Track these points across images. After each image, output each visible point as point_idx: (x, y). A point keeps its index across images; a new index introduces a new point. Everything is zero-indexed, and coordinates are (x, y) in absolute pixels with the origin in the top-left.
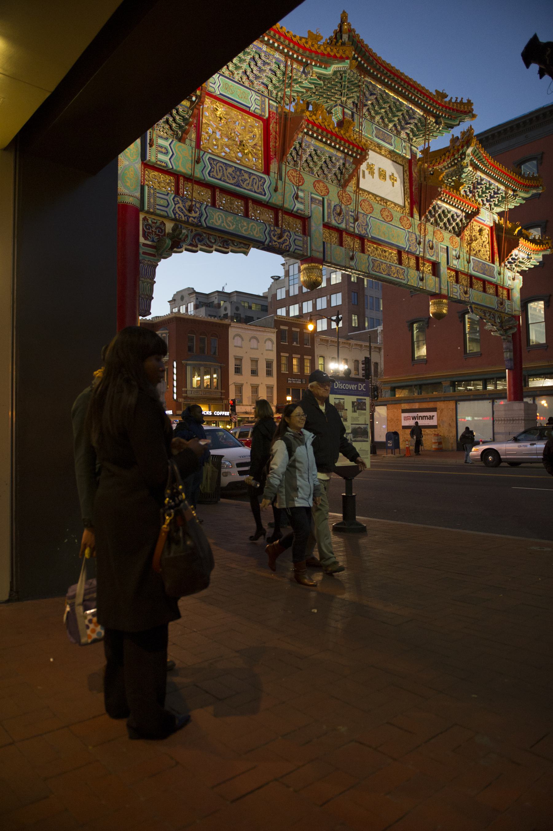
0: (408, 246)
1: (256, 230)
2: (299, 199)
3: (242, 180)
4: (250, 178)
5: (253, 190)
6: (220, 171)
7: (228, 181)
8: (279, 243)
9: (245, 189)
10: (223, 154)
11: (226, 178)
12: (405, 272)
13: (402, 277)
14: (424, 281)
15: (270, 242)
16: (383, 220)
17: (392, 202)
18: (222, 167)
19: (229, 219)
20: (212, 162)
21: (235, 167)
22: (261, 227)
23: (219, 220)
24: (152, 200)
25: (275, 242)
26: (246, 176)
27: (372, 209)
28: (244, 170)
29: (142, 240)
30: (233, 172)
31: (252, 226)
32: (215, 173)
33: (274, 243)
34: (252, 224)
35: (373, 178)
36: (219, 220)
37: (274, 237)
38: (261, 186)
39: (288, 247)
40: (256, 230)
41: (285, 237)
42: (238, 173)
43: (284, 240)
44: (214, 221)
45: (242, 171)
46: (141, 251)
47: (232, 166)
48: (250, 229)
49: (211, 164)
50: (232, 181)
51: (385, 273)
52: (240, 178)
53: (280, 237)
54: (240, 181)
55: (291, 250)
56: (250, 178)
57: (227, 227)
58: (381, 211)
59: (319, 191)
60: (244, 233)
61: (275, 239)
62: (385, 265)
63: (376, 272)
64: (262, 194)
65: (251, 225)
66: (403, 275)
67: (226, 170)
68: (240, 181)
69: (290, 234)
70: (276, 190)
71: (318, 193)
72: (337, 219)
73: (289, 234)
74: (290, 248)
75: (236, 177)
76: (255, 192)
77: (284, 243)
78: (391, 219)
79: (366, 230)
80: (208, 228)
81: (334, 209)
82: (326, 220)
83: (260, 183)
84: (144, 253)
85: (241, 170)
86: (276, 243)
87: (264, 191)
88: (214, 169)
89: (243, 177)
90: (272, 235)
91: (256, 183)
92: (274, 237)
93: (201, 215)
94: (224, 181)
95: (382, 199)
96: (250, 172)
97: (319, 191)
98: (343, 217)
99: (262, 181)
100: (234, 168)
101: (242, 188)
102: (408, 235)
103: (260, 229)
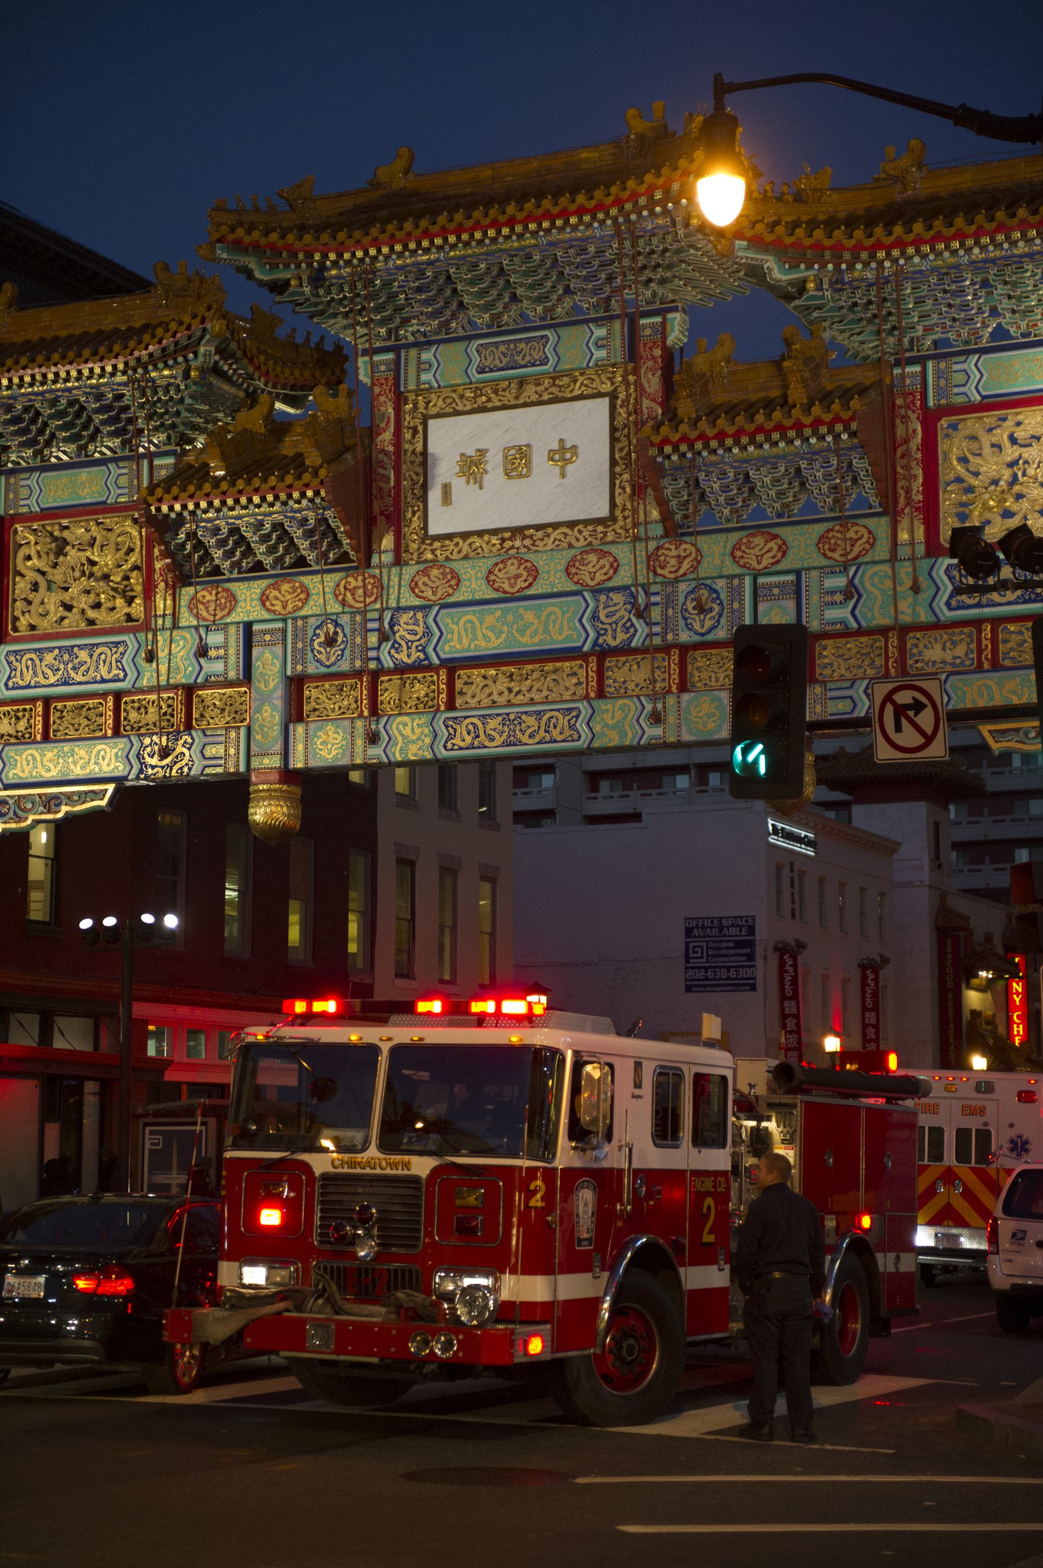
0: (592, 635)
1: (107, 760)
2: (212, 653)
3: (74, 668)
4: (91, 656)
5: (99, 678)
6: (28, 668)
7: (43, 682)
8: (162, 767)
9: (80, 683)
11: (41, 679)
12: (577, 717)
13: (567, 733)
14: (671, 719)
15: (141, 771)
16: (501, 595)
18: (31, 659)
19: (49, 755)
20: (12, 658)
21: (60, 648)
22: (121, 746)
23: (28, 765)
25: (153, 767)
26: (83, 655)
27: (453, 582)
28: (78, 646)
30: (55, 659)
31: (99, 752)
32: (17, 680)
33: (150, 771)
34: (99, 747)
35: (481, 488)
36: (28, 765)
37: (152, 757)
38: (117, 662)
39: (186, 770)
40: (107, 760)
41: (180, 749)
42: (66, 657)
43: (177, 757)
44: (18, 771)
45: (76, 650)
47: (54, 648)
48: (93, 761)
49: (9, 663)
50: (53, 680)
51: (499, 741)
52: (70, 665)
53: (163, 757)
54: (70, 671)
55: (192, 773)
56: (91, 656)
57: (43, 773)
58: (490, 572)
59: (278, 607)
61: (154, 761)
62: (500, 718)
63: (461, 748)
64: (119, 680)
65: (95, 752)
66: (572, 727)
67: (41, 660)
68: (70, 671)
69: (192, 738)
71: (274, 612)
72: (323, 657)
73: (190, 740)
74: (190, 769)
75: (62, 666)
76: (104, 681)
77: (176, 763)
78: (531, 579)
79: (423, 651)
81: (315, 635)
83: (115, 656)
85: (73, 647)
86: (156, 770)
87: (124, 670)
88: (15, 670)
89: (76, 661)
90: (146, 756)
91: (104, 662)
92: (152, 757)
94: (35, 687)
96: (91, 645)
97: (278, 607)
98: (342, 647)
99: (121, 649)
100: (57, 651)
101: (74, 684)
102: (592, 604)
103: (116, 754)
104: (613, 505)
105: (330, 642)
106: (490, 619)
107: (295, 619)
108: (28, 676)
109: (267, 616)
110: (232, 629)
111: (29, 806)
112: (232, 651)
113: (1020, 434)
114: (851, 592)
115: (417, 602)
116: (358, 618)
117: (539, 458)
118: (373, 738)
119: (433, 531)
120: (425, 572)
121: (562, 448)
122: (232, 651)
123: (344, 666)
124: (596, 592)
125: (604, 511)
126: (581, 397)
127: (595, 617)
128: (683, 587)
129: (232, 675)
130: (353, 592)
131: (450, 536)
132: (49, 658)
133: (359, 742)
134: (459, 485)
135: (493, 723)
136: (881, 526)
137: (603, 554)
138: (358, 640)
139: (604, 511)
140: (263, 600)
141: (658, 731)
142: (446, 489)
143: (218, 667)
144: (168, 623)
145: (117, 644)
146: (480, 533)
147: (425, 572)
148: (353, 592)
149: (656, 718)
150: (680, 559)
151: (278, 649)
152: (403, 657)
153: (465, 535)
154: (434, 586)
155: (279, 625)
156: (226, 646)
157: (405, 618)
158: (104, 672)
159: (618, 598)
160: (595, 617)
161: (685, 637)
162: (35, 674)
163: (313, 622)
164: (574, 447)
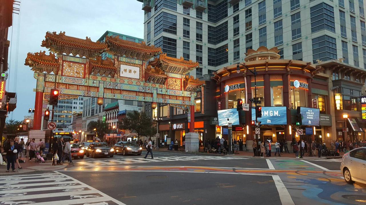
10: (70, 75)
14: (145, 99)
17: (134, 78)
24: (47, 90)
26: (76, 80)
29: (44, 99)
41: (90, 93)
46: (43, 102)
53: (87, 94)
59: (103, 80)
60: (74, 94)
61: (86, 94)
70: (86, 82)
76: (79, 84)
80: (63, 94)
82: (105, 87)
84: (44, 102)
93: (61, 91)
95: (129, 78)
97: (103, 80)
104: (139, 78)
105: (110, 85)
106: (128, 86)
107: (106, 82)
108: (68, 81)
109: (101, 80)
110: (97, 81)
111: (65, 97)
112: (97, 84)
113: (173, 80)
114: (162, 91)
115: (119, 83)
116: (113, 83)
117: (132, 71)
118: (114, 96)
119: (121, 76)
120: (121, 80)
121: (135, 71)
122: (97, 84)
123: (111, 88)
124: (139, 86)
125: (139, 78)
126: (137, 67)
127: (139, 88)
128: (147, 87)
129: (97, 86)
130: (112, 80)
131: (123, 77)
132: (71, 79)
133: (113, 96)
134: (124, 72)
135: (128, 97)
136: (163, 85)
137: (139, 82)
138: (113, 85)
139: (139, 78)
140: (101, 79)
141: (144, 100)
142: (122, 72)
143: (96, 85)
144: (88, 78)
145: (81, 80)
146: (126, 77)
147: (121, 80)
148: (112, 80)
149: (144, 99)
150: (147, 85)
151: (103, 85)
152: (118, 88)
153: (124, 77)
154: (122, 81)
155: (103, 82)
156: (96, 83)
157: (119, 84)
158: (79, 82)
159: (141, 87)
160: (139, 88)
161: (147, 92)
162: (69, 81)
163: (108, 82)
164: (136, 71)
